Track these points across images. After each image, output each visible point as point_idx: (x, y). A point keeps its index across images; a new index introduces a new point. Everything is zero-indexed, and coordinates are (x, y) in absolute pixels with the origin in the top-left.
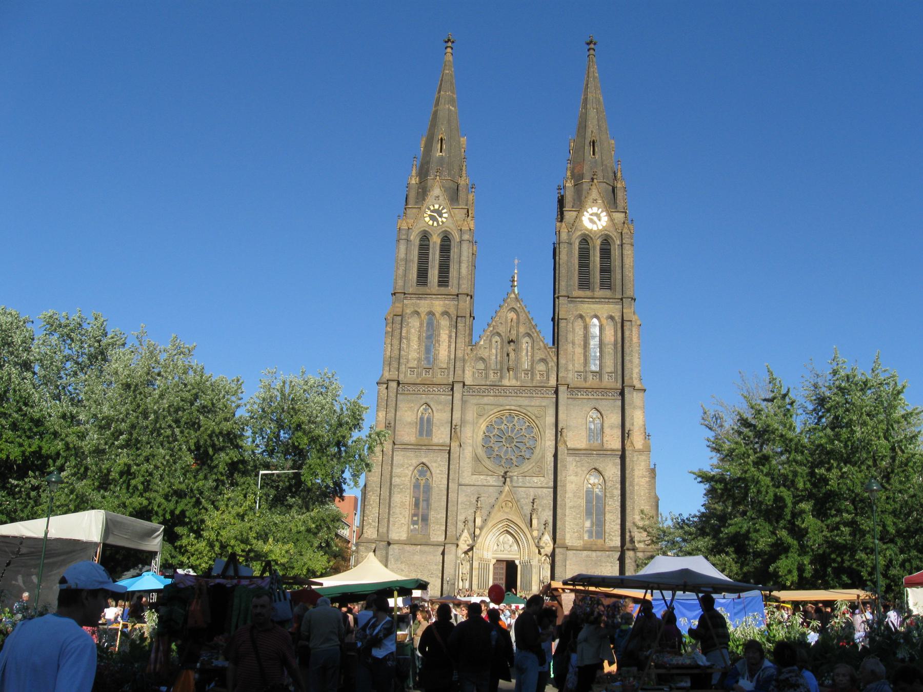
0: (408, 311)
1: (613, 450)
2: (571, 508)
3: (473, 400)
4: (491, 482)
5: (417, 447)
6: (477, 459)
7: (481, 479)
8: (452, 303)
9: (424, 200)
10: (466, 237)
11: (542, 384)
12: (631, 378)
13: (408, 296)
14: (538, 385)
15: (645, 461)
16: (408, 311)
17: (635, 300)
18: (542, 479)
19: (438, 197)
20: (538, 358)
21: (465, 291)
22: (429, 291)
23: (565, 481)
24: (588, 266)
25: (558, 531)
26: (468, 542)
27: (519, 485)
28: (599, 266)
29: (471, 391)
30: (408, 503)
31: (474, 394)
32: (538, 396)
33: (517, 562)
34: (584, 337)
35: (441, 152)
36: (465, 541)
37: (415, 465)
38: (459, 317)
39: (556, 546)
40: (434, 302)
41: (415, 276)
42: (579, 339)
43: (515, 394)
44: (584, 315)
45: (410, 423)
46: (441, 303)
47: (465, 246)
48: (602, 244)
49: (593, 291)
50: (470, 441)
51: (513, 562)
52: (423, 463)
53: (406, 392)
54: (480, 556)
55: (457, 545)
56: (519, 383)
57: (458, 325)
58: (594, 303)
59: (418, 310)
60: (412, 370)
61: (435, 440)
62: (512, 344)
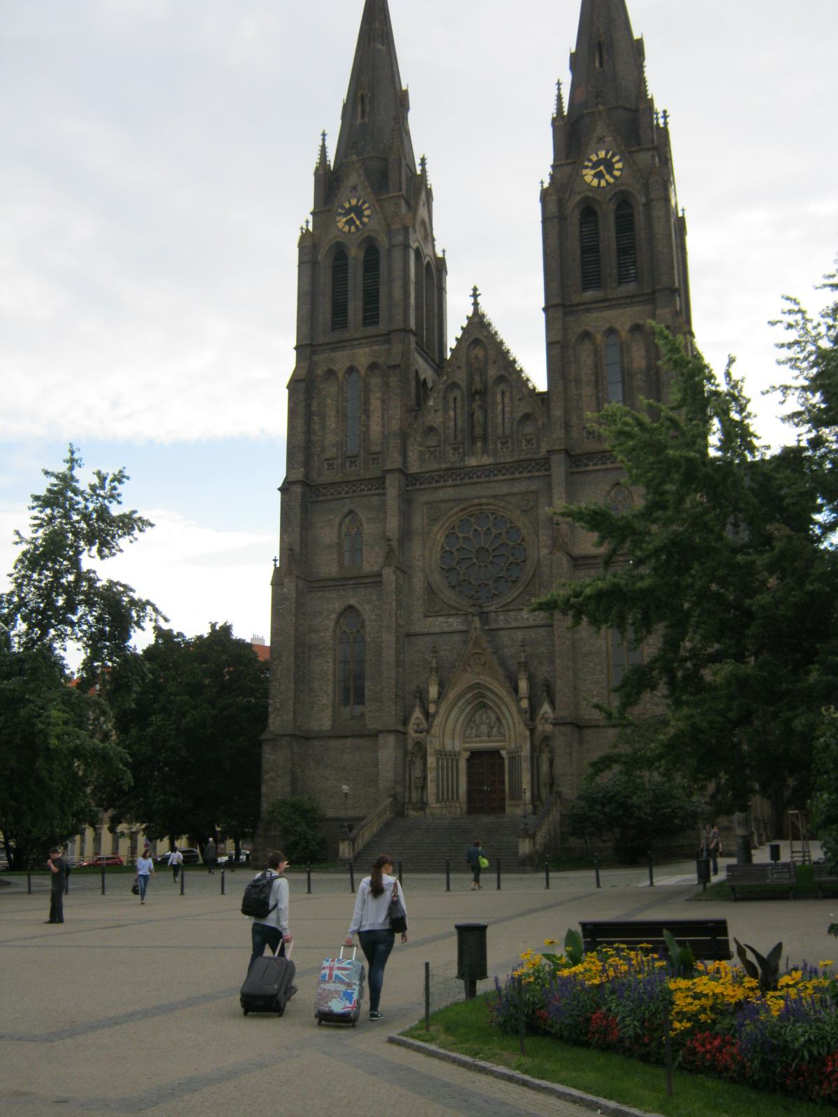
0: (320, 371)
3: (423, 498)
4: (455, 625)
5: (341, 582)
6: (431, 591)
7: (438, 624)
8: (383, 347)
10: (399, 239)
11: (530, 456)
13: (319, 348)
14: (522, 457)
16: (320, 371)
19: (354, 188)
20: (521, 414)
21: (402, 326)
22: (347, 336)
24: (595, 249)
26: (421, 727)
27: (499, 626)
28: (614, 245)
29: (418, 483)
30: (331, 672)
31: (423, 486)
32: (523, 475)
33: (503, 753)
34: (596, 367)
35: (363, 116)
36: (418, 725)
37: (339, 610)
38: (389, 367)
40: (356, 351)
41: (329, 316)
42: (586, 373)
43: (487, 479)
44: (592, 330)
46: (367, 350)
48: (619, 207)
52: (350, 608)
53: (322, 498)
54: (438, 748)
55: (405, 734)
58: (606, 308)
59: (335, 368)
60: (331, 462)
61: (367, 568)
62: (477, 397)
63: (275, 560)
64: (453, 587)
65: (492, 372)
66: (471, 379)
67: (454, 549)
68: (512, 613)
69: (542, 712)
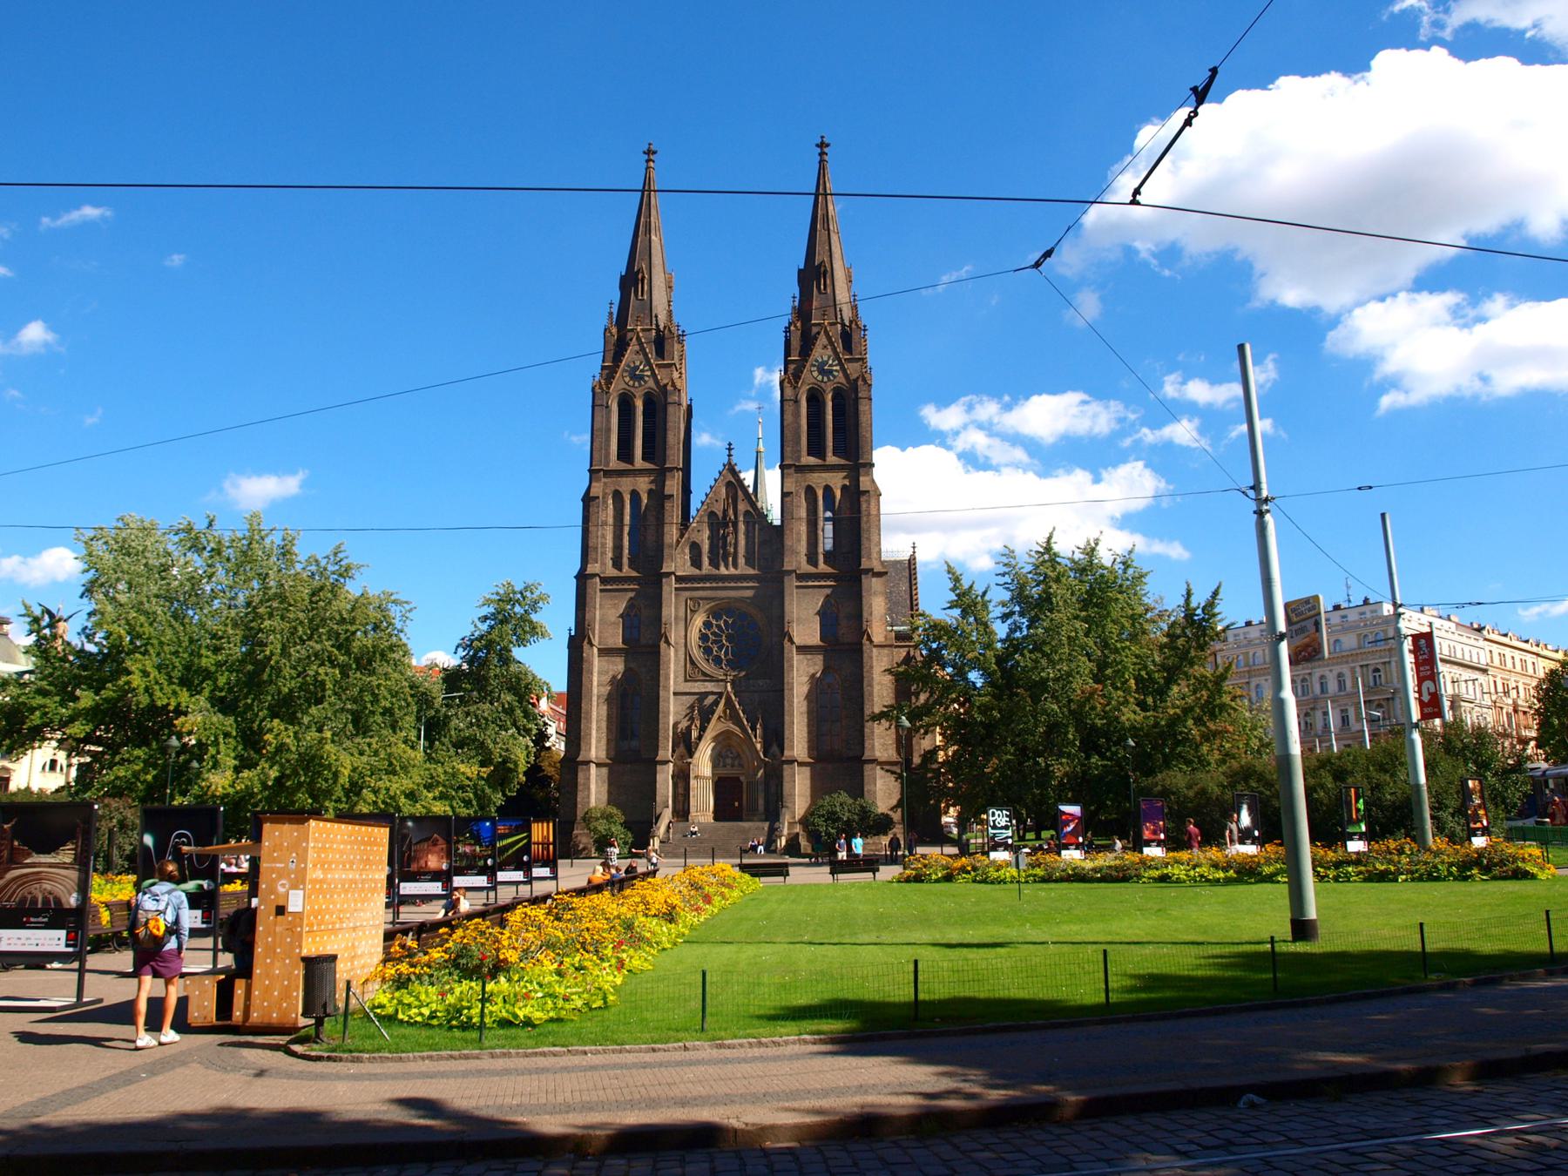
9: (624, 356)
12: (869, 558)
15: (888, 655)
18: (768, 681)
22: (630, 467)
28: (831, 425)
33: (742, 778)
35: (642, 295)
46: (646, 479)
47: (671, 409)
51: (738, 778)
59: (620, 490)
61: (643, 641)
63: (570, 630)
64: (708, 660)
65: (743, 506)
66: (725, 511)
67: (709, 633)
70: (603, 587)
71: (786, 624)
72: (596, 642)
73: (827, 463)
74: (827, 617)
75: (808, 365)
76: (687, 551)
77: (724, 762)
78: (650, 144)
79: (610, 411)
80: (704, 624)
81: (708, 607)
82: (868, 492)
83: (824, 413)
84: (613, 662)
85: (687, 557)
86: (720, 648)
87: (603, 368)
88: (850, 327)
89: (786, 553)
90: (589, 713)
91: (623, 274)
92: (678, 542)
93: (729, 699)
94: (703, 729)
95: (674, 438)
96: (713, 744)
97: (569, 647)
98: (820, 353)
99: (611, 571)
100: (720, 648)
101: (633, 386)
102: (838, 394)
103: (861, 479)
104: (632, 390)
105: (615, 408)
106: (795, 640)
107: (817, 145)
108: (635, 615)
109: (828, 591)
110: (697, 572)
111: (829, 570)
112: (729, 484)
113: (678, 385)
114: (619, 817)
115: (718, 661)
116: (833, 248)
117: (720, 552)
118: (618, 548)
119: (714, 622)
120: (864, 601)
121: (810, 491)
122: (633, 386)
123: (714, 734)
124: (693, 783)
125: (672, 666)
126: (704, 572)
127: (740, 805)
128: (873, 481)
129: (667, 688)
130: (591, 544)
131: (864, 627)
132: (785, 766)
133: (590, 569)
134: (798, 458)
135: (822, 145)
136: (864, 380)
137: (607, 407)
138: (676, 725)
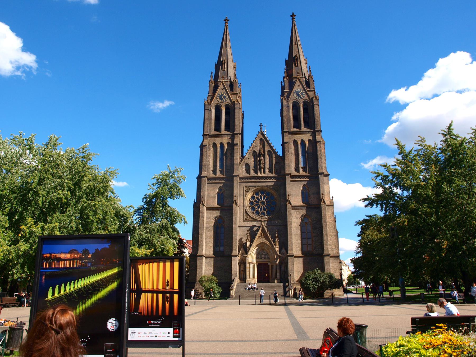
1: (314, 205)
2: (295, 235)
9: (217, 91)
12: (322, 168)
15: (332, 210)
17: (321, 131)
19: (223, 89)
22: (220, 133)
23: (291, 221)
25: (289, 247)
33: (269, 264)
35: (224, 69)
39: (288, 254)
40: (223, 138)
44: (297, 140)
45: (213, 197)
46: (226, 138)
47: (236, 111)
49: (300, 129)
50: (243, 204)
51: (267, 264)
56: (266, 174)
57: (235, 148)
59: (216, 142)
61: (225, 204)
63: (194, 200)
65: (267, 148)
66: (260, 151)
68: (272, 221)
69: (282, 251)
70: (208, 182)
71: (287, 196)
72: (205, 204)
73: (302, 131)
74: (305, 195)
75: (292, 93)
76: (244, 167)
77: (261, 256)
78: (226, 17)
79: (211, 112)
80: (251, 197)
81: (253, 190)
82: (320, 141)
83: (300, 111)
84: (213, 213)
85: (244, 169)
86: (259, 207)
87: (209, 96)
88: (309, 79)
89: (286, 167)
90: (202, 235)
91: (216, 63)
92: (240, 163)
93: (263, 228)
94: (252, 242)
95: (238, 122)
96: (257, 248)
97: (193, 207)
98: (298, 88)
99: (212, 175)
100: (259, 207)
101: (221, 102)
102: (305, 104)
103: (317, 136)
104: (221, 103)
105: (213, 110)
106: (292, 203)
107: (291, 16)
108: (222, 194)
109: (305, 183)
110: (248, 175)
111: (304, 174)
112: (261, 140)
113: (239, 101)
114: (215, 280)
115: (258, 213)
116: (299, 51)
117: (258, 167)
118: (215, 166)
119: (256, 196)
120: (321, 187)
121: (295, 142)
122: (221, 102)
123: (257, 244)
124: (248, 265)
125: (238, 214)
126: (251, 175)
127: (269, 275)
128: (321, 138)
129: (236, 224)
130: (203, 164)
131: (321, 197)
132: (289, 258)
133: (203, 174)
134: (290, 129)
135: (293, 16)
136: (316, 98)
137: (210, 110)
138: (241, 240)
